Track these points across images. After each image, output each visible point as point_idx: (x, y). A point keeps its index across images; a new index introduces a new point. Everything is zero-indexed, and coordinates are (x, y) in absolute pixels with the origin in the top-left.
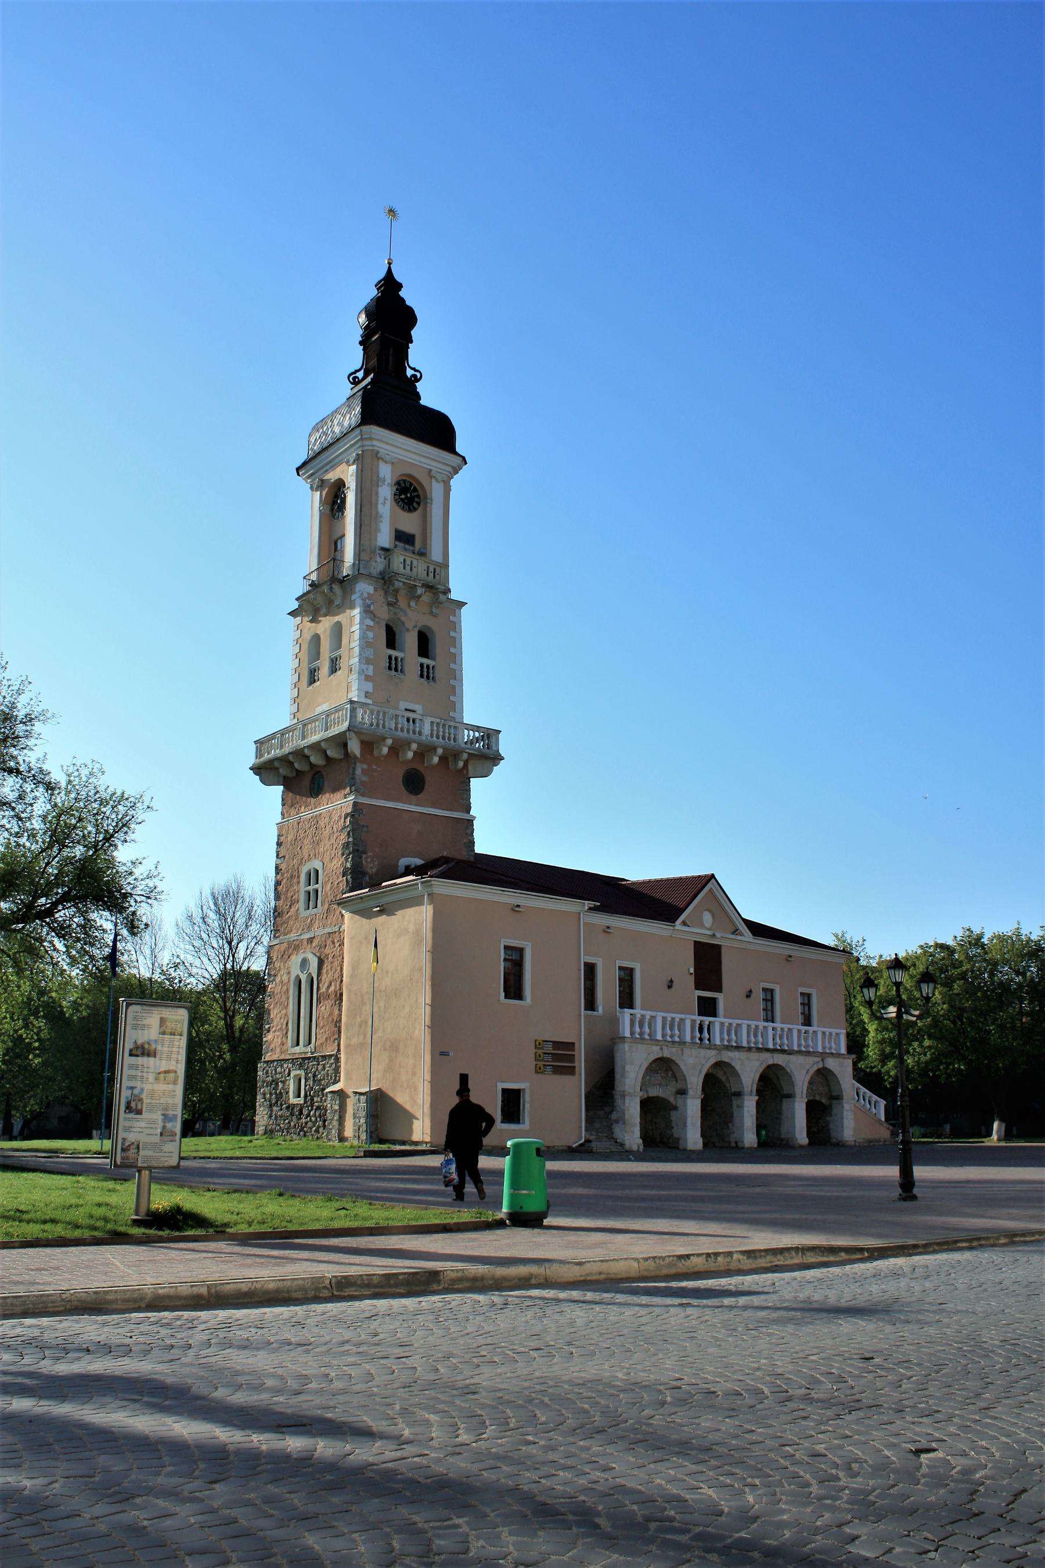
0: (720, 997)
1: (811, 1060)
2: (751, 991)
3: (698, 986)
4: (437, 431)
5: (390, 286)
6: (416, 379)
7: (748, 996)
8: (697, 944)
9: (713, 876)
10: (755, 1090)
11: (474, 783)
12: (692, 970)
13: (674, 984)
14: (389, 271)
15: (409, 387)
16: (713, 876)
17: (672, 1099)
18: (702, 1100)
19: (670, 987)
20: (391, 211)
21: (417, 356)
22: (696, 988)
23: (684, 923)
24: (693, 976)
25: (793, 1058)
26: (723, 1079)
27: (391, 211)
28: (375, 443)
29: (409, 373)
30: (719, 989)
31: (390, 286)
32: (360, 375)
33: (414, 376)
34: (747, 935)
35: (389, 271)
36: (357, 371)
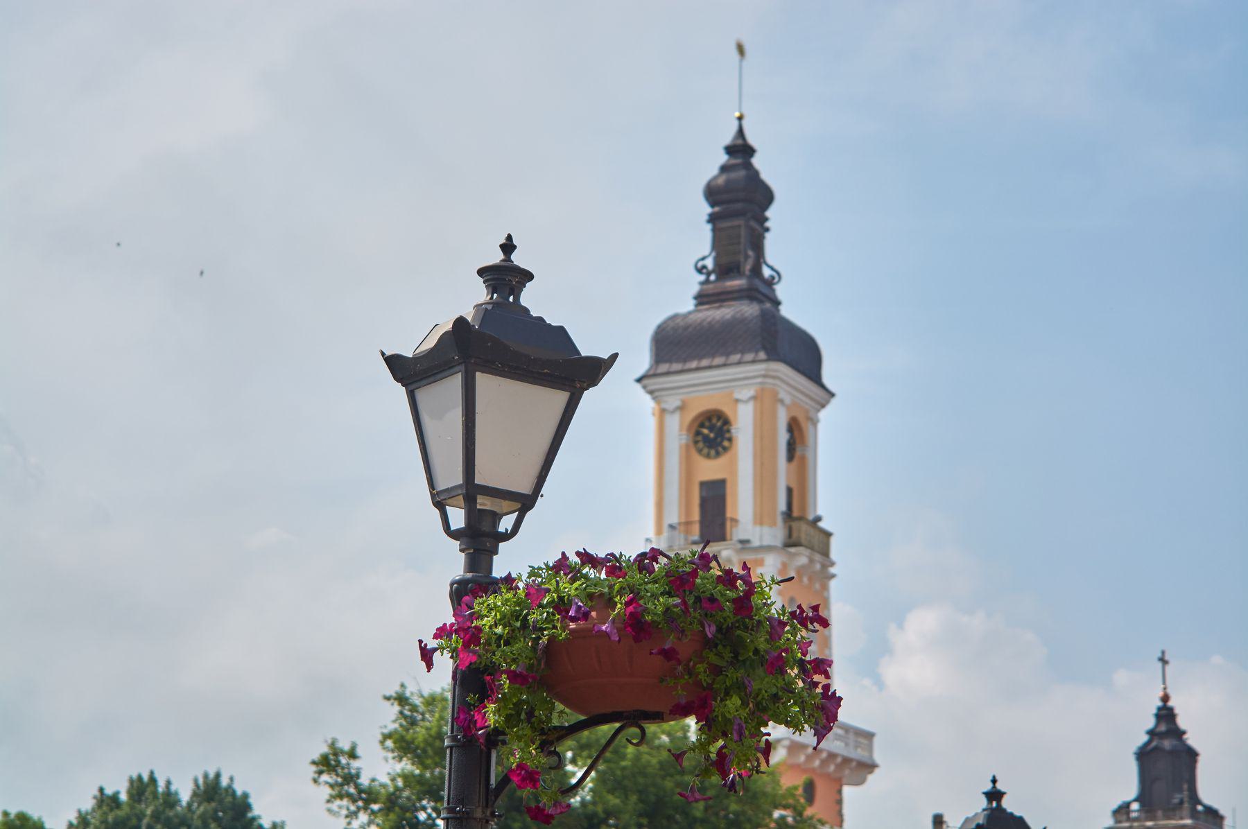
4: (804, 355)
5: (740, 150)
6: (770, 283)
11: (847, 790)
14: (741, 132)
15: (762, 291)
20: (741, 49)
21: (776, 250)
27: (741, 49)
28: (778, 382)
29: (767, 272)
31: (740, 150)
32: (709, 263)
33: (773, 278)
35: (741, 132)
36: (703, 259)
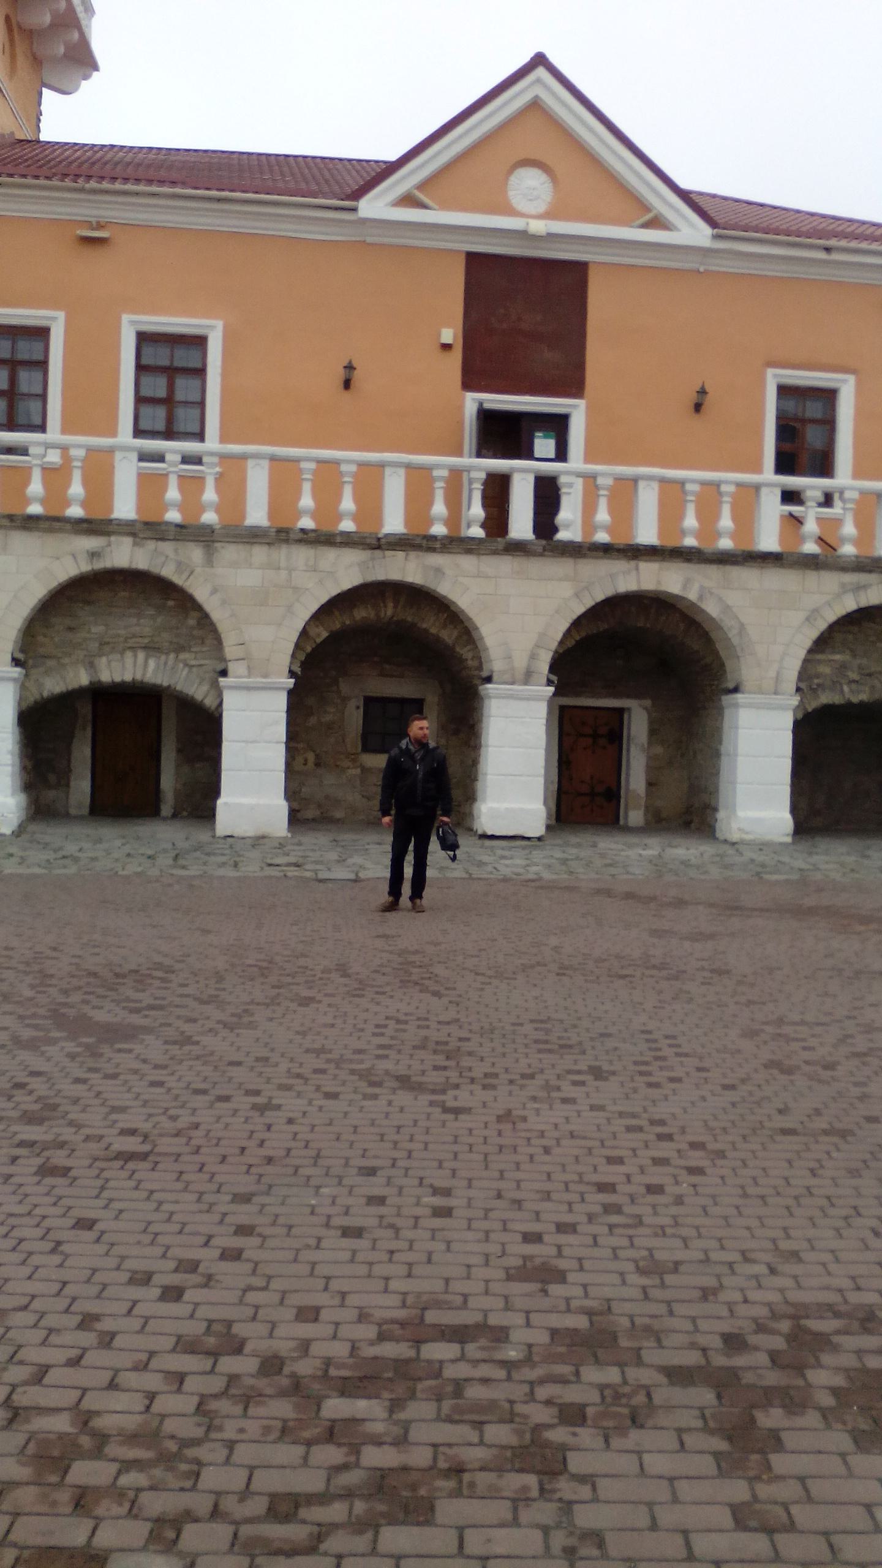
0: (578, 413)
1: (830, 581)
2: (703, 392)
3: (471, 380)
7: (698, 407)
8: (474, 260)
9: (540, 60)
10: (545, 668)
12: (447, 335)
13: (357, 375)
16: (540, 60)
17: (198, 691)
18: (291, 693)
19: (347, 384)
22: (469, 384)
23: (408, 200)
24: (457, 355)
25: (747, 576)
26: (448, 636)
30: (574, 386)
34: (693, 232)
